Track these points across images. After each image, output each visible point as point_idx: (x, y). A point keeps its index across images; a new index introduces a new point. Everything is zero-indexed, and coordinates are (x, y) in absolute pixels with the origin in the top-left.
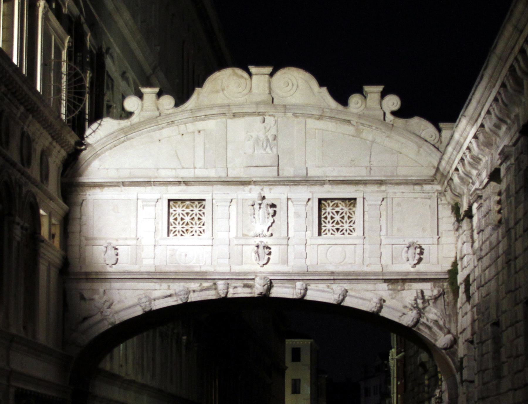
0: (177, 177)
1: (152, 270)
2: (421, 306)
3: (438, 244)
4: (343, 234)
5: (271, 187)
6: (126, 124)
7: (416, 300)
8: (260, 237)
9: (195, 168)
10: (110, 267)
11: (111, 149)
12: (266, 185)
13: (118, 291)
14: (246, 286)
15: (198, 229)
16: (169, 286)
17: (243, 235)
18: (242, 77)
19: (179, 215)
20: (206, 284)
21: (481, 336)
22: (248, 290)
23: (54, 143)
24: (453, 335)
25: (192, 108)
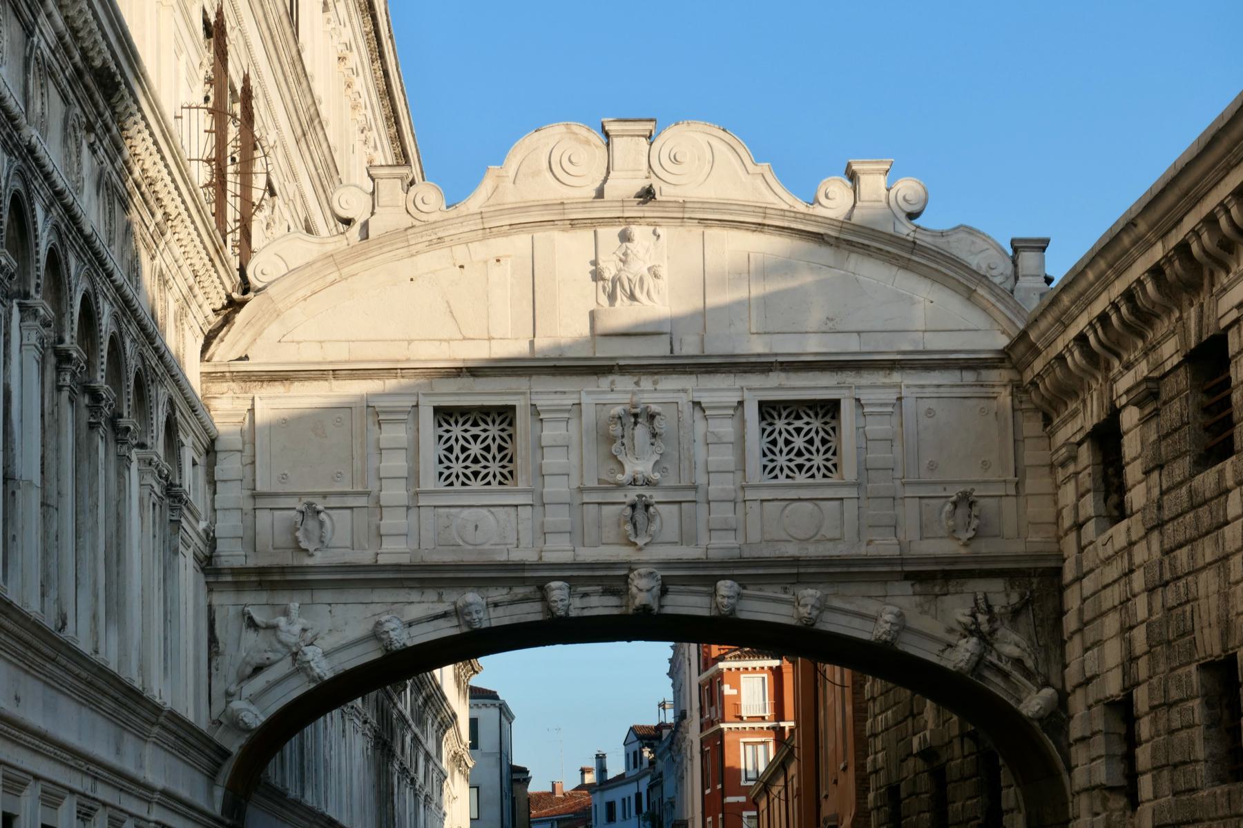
0: (455, 360)
1: (405, 560)
2: (985, 628)
3: (1017, 495)
4: (813, 476)
5: (656, 377)
6: (338, 245)
7: (973, 615)
8: (635, 485)
10: (311, 555)
12: (644, 374)
13: (329, 608)
14: (607, 592)
15: (498, 470)
16: (440, 595)
17: (599, 480)
18: (587, 142)
19: (457, 440)
20: (520, 591)
21: (1166, 691)
22: (613, 601)
24: (1057, 690)
25: (483, 210)
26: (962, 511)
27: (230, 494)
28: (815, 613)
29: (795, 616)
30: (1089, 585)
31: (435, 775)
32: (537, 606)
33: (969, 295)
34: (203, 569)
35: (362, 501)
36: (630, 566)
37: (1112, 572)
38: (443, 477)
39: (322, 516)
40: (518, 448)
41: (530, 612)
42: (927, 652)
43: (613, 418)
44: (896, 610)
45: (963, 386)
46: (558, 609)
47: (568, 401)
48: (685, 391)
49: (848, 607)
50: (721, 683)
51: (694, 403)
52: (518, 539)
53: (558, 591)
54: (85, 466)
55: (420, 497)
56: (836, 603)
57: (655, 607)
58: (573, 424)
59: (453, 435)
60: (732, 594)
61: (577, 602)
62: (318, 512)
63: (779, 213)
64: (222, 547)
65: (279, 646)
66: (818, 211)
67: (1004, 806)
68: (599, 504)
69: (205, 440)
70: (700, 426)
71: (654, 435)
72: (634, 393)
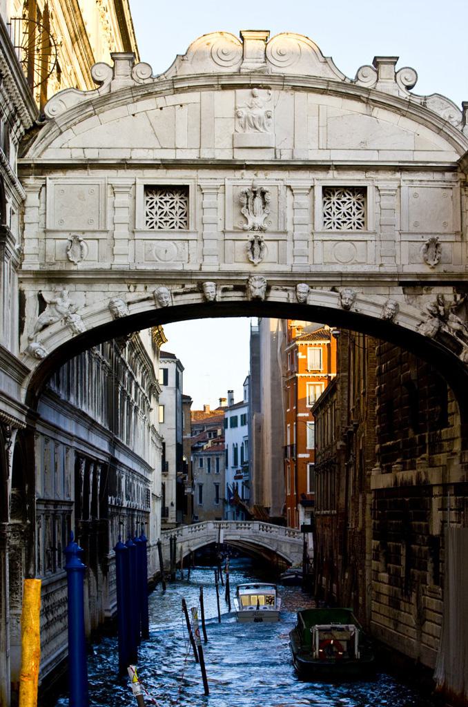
0: (156, 160)
1: (126, 268)
2: (442, 313)
5: (266, 172)
9: (176, 148)
10: (76, 265)
11: (75, 124)
14: (236, 288)
16: (146, 288)
22: (240, 294)
23: (16, 117)
26: (432, 249)
27: (31, 231)
28: (350, 303)
29: (340, 304)
31: (141, 396)
32: (198, 296)
33: (439, 131)
34: (17, 271)
35: (103, 236)
36: (250, 274)
38: (148, 224)
39: (82, 243)
40: (190, 208)
41: (195, 299)
42: (410, 325)
43: (243, 193)
44: (394, 302)
45: (434, 181)
46: (210, 297)
47: (218, 183)
48: (282, 180)
49: (369, 300)
50: (297, 352)
51: (287, 186)
52: (189, 258)
53: (210, 288)
55: (136, 234)
56: (361, 297)
57: (263, 297)
58: (221, 196)
59: (154, 201)
60: (305, 291)
61: (220, 294)
62: (80, 241)
63: (336, 84)
64: (27, 259)
65: (57, 314)
66: (359, 83)
67: (449, 412)
68: (233, 240)
69: (19, 201)
71: (265, 203)
72: (254, 180)
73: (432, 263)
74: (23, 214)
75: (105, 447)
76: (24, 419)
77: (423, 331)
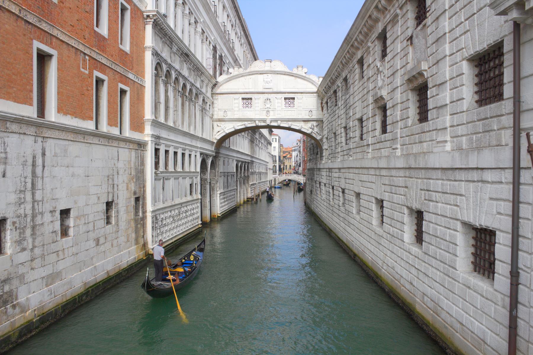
20: (252, 122)
22: (264, 123)
26: (310, 112)
27: (216, 109)
30: (325, 122)
33: (313, 83)
36: (266, 119)
37: (327, 121)
41: (254, 125)
47: (259, 97)
53: (257, 122)
54: (185, 106)
66: (293, 72)
70: (276, 101)
73: (311, 116)
74: (213, 105)
75: (249, 158)
76: (214, 154)
77: (308, 132)
